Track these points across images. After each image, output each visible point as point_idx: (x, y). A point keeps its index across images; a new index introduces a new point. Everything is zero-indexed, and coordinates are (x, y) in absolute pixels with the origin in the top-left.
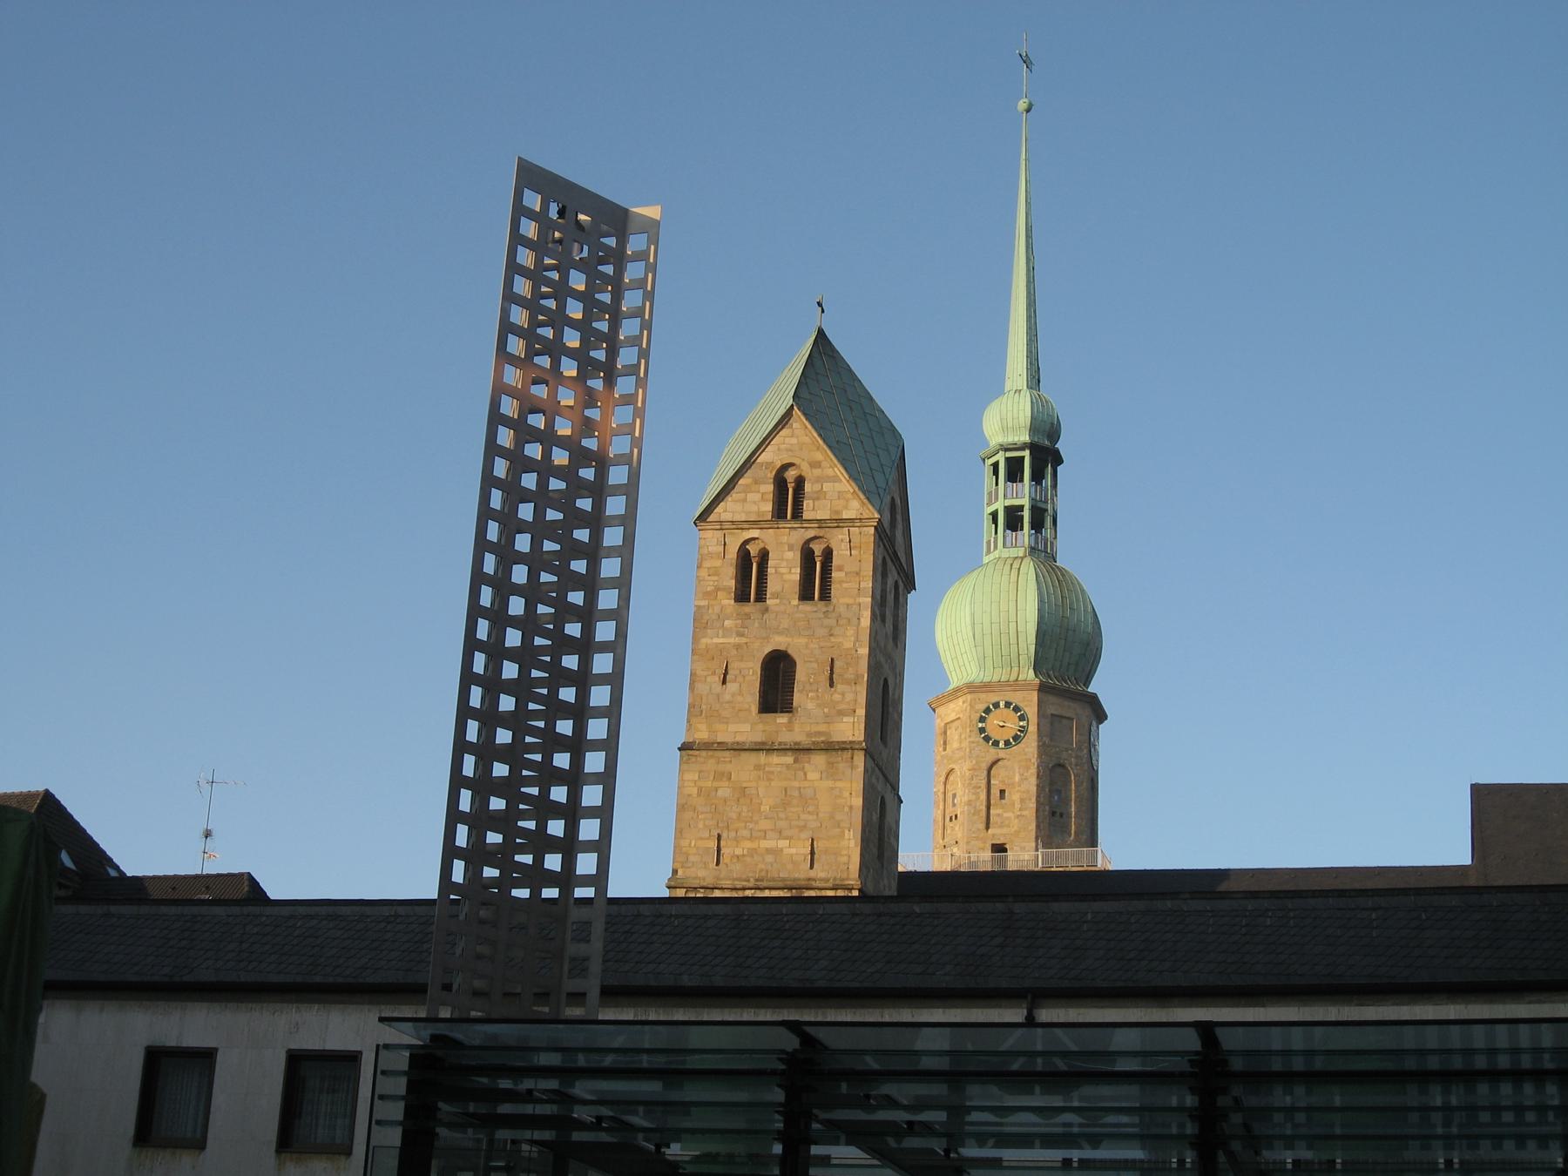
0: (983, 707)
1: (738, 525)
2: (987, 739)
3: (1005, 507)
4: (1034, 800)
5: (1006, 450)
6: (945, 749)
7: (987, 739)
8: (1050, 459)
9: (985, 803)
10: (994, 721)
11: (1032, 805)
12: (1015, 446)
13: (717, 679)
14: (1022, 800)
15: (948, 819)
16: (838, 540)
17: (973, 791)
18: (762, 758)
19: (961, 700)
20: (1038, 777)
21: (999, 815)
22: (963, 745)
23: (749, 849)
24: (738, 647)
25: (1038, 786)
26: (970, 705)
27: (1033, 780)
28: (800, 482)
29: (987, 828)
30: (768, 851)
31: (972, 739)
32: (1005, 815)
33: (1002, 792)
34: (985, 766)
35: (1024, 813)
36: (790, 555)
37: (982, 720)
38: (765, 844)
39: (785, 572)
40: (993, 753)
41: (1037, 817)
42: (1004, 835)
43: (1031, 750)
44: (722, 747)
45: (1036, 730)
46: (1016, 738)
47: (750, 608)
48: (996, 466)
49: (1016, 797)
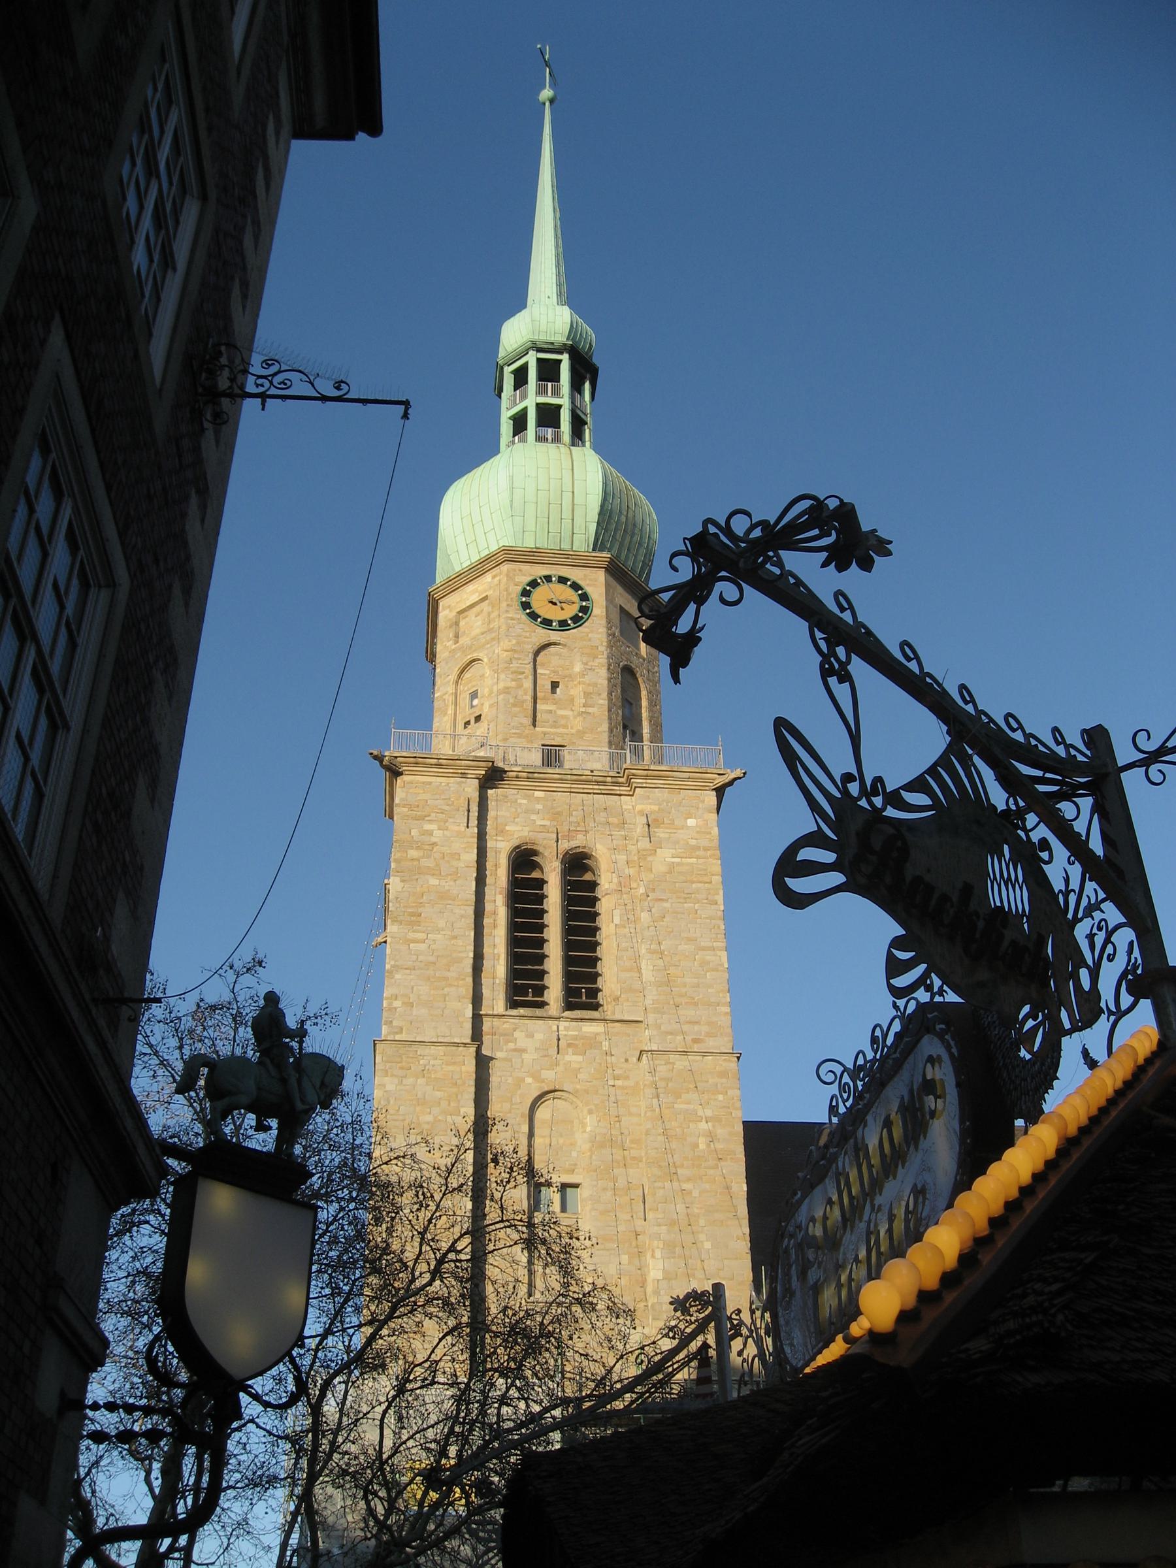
0: (529, 579)
2: (534, 616)
3: (537, 404)
4: (605, 695)
5: (540, 350)
6: (456, 642)
7: (534, 616)
8: (588, 376)
9: (530, 693)
10: (539, 600)
11: (603, 701)
12: (550, 347)
14: (587, 695)
15: (460, 725)
17: (511, 676)
19: (488, 578)
20: (609, 669)
21: (550, 712)
22: (495, 625)
25: (609, 680)
26: (507, 575)
27: (604, 673)
29: (534, 725)
31: (510, 616)
33: (555, 685)
34: (530, 648)
35: (590, 710)
37: (525, 593)
40: (542, 635)
41: (610, 718)
42: (561, 735)
43: (600, 636)
45: (605, 614)
46: (576, 619)
49: (577, 691)
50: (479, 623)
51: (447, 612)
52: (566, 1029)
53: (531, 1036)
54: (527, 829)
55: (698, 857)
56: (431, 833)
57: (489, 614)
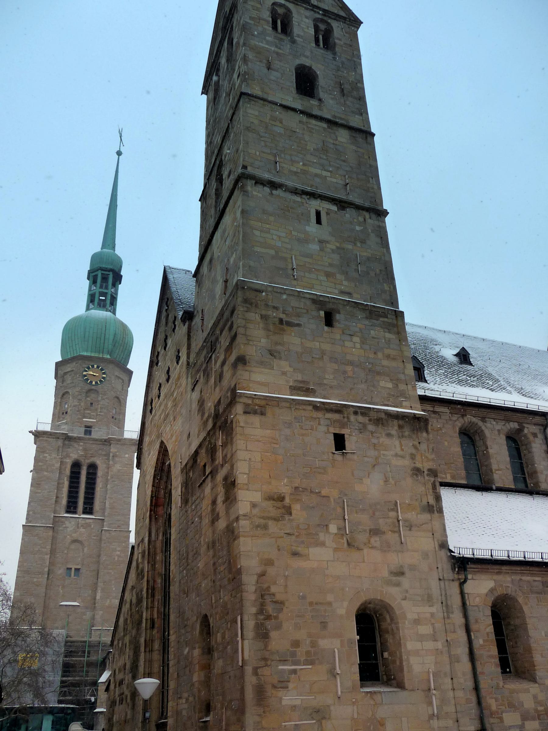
0: (87, 366)
3: (99, 292)
6: (62, 384)
15: (61, 413)
21: (89, 413)
23: (301, 170)
32: (92, 414)
50: (70, 378)
51: (60, 371)
52: (81, 521)
53: (70, 523)
54: (76, 455)
55: (127, 467)
56: (46, 457)
57: (73, 377)
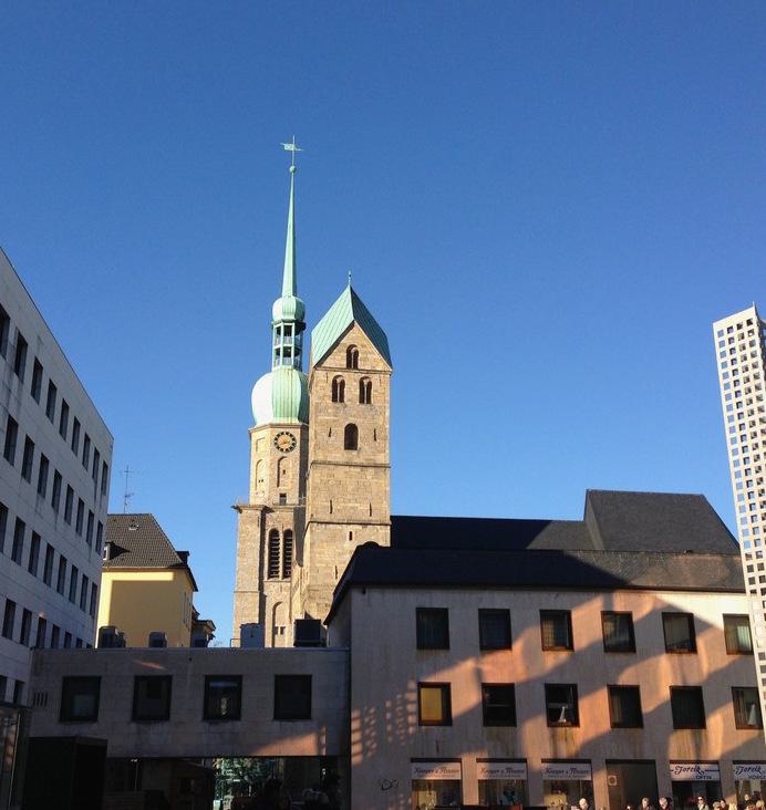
1: (334, 370)
2: (278, 448)
10: (281, 440)
13: (325, 435)
16: (375, 379)
18: (347, 468)
24: (334, 421)
28: (357, 353)
30: (352, 508)
36: (355, 384)
38: (350, 505)
39: (352, 391)
40: (281, 454)
44: (330, 463)
46: (291, 448)
47: (338, 405)
48: (279, 329)
49: (290, 473)
